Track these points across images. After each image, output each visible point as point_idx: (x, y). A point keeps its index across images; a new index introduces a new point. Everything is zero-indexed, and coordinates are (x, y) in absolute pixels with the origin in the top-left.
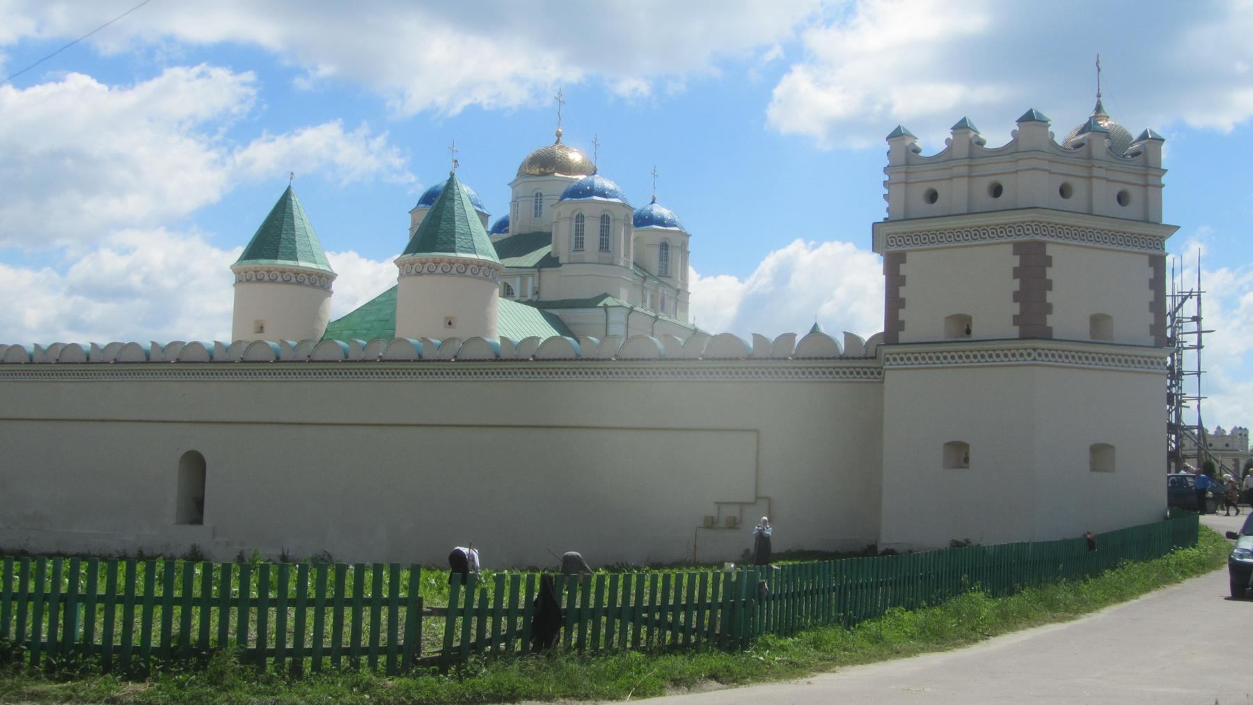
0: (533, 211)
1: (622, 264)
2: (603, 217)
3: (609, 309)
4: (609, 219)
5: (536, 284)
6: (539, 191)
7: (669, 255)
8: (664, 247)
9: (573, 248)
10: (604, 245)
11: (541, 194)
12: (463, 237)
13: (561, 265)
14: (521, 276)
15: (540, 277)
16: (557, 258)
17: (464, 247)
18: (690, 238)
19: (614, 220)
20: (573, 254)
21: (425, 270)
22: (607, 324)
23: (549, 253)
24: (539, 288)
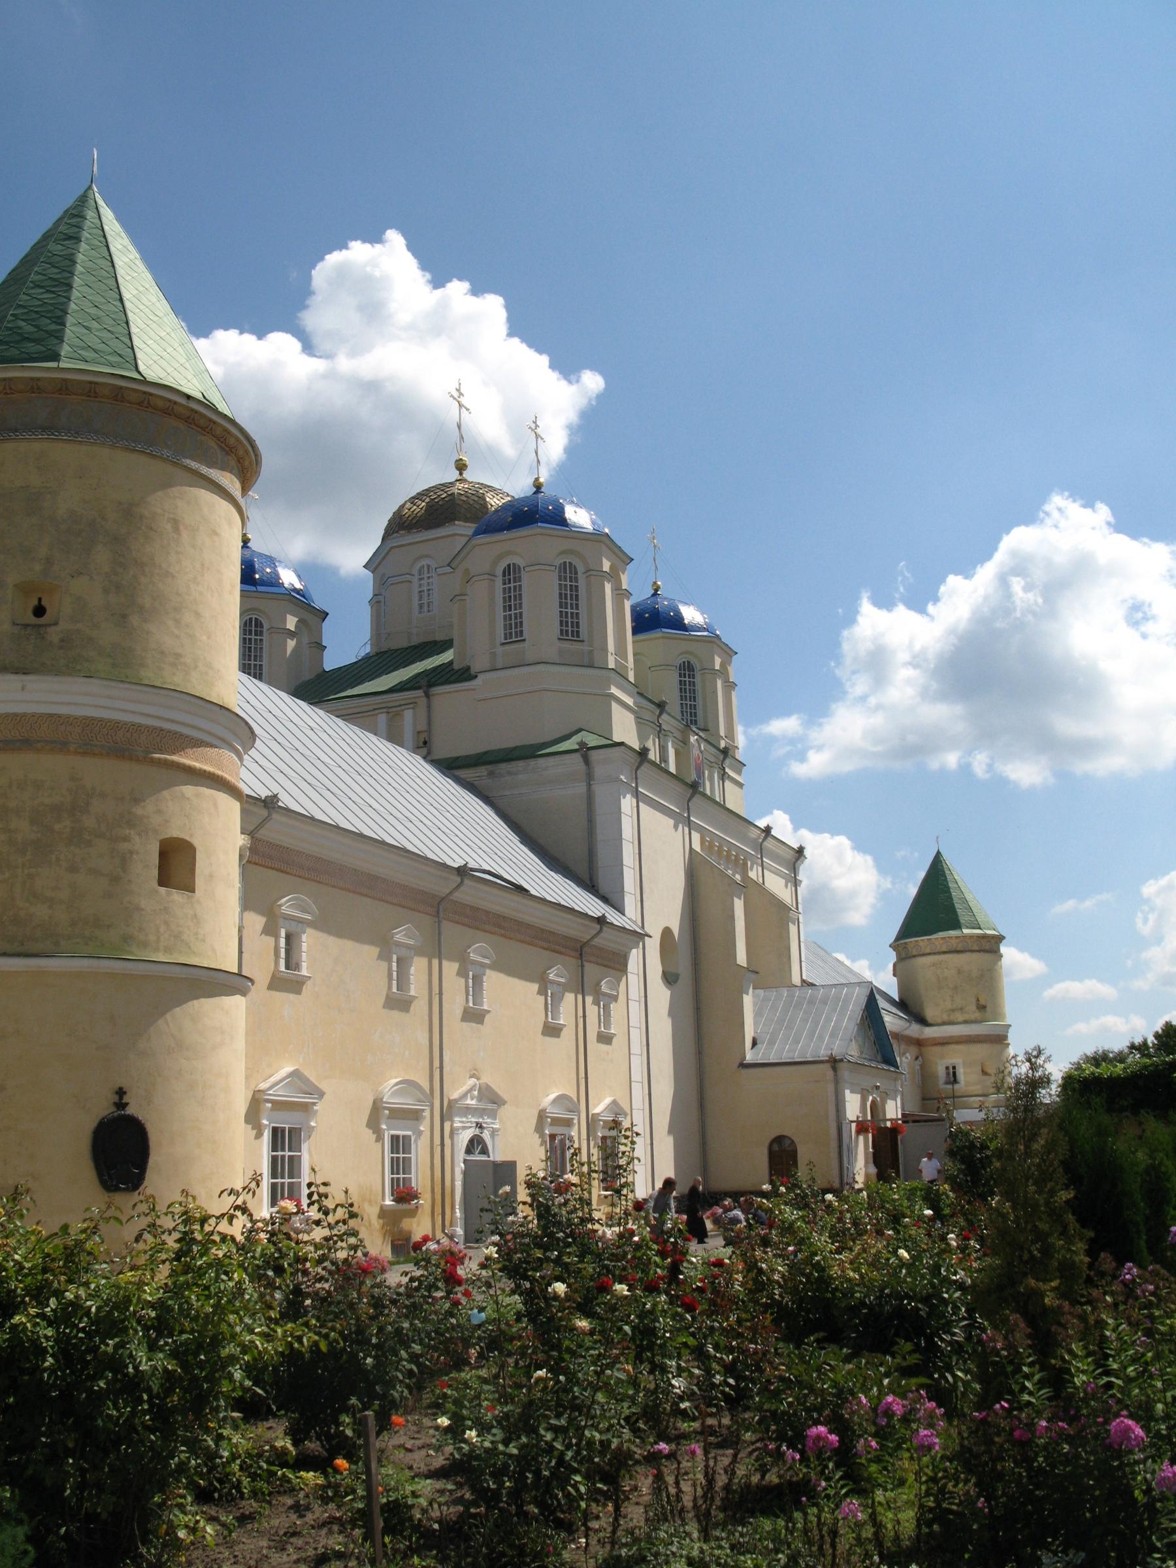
0: (416, 602)
1: (611, 665)
3: (594, 755)
4: (576, 573)
5: (422, 726)
6: (424, 562)
7: (698, 687)
8: (687, 670)
10: (570, 628)
11: (428, 566)
12: (94, 325)
13: (476, 676)
14: (388, 709)
15: (429, 707)
16: (468, 669)
17: (95, 351)
18: (735, 658)
20: (500, 650)
23: (451, 663)
24: (429, 731)
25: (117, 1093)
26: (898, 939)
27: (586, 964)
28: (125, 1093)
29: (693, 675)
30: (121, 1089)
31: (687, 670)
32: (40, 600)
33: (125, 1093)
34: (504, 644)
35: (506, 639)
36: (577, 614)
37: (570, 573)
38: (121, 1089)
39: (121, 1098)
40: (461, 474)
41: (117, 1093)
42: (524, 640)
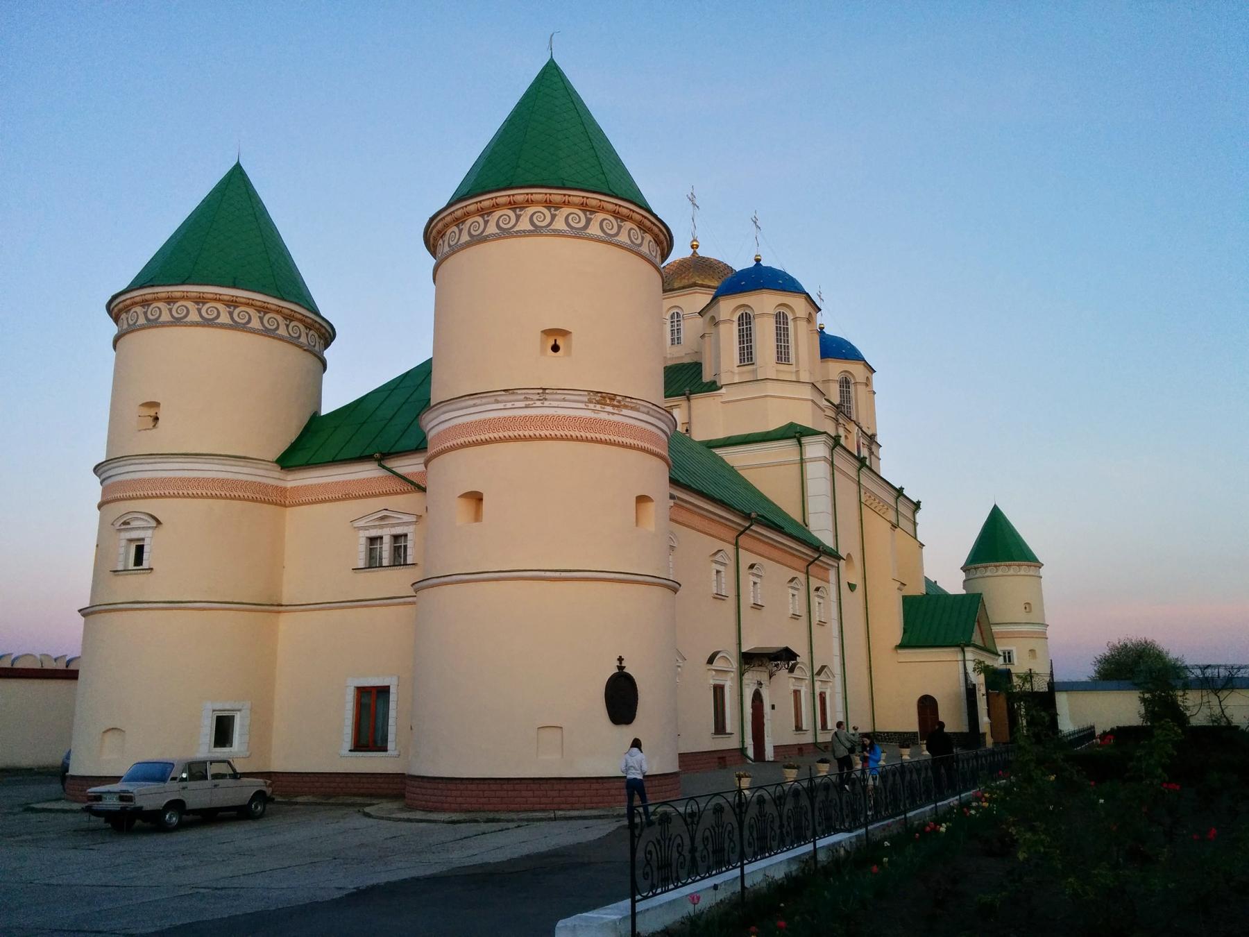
2: (778, 316)
3: (804, 440)
4: (787, 319)
6: (675, 310)
7: (853, 394)
8: (845, 383)
9: (737, 362)
10: (783, 355)
11: (677, 313)
13: (722, 387)
16: (714, 382)
19: (795, 319)
21: (492, 229)
22: (802, 461)
25: (618, 659)
26: (966, 564)
27: (810, 577)
28: (623, 659)
29: (849, 386)
30: (620, 657)
31: (845, 383)
32: (555, 341)
33: (623, 659)
34: (738, 366)
35: (741, 362)
36: (788, 346)
37: (783, 319)
38: (620, 657)
39: (621, 663)
40: (695, 252)
41: (618, 659)
42: (753, 364)
